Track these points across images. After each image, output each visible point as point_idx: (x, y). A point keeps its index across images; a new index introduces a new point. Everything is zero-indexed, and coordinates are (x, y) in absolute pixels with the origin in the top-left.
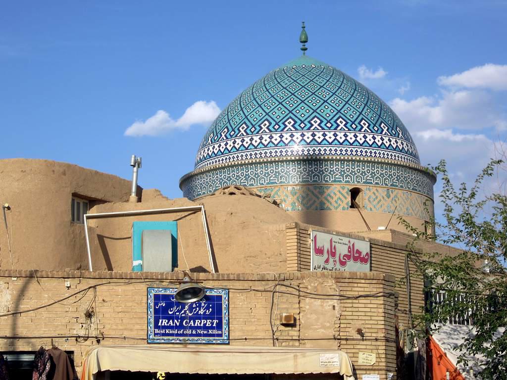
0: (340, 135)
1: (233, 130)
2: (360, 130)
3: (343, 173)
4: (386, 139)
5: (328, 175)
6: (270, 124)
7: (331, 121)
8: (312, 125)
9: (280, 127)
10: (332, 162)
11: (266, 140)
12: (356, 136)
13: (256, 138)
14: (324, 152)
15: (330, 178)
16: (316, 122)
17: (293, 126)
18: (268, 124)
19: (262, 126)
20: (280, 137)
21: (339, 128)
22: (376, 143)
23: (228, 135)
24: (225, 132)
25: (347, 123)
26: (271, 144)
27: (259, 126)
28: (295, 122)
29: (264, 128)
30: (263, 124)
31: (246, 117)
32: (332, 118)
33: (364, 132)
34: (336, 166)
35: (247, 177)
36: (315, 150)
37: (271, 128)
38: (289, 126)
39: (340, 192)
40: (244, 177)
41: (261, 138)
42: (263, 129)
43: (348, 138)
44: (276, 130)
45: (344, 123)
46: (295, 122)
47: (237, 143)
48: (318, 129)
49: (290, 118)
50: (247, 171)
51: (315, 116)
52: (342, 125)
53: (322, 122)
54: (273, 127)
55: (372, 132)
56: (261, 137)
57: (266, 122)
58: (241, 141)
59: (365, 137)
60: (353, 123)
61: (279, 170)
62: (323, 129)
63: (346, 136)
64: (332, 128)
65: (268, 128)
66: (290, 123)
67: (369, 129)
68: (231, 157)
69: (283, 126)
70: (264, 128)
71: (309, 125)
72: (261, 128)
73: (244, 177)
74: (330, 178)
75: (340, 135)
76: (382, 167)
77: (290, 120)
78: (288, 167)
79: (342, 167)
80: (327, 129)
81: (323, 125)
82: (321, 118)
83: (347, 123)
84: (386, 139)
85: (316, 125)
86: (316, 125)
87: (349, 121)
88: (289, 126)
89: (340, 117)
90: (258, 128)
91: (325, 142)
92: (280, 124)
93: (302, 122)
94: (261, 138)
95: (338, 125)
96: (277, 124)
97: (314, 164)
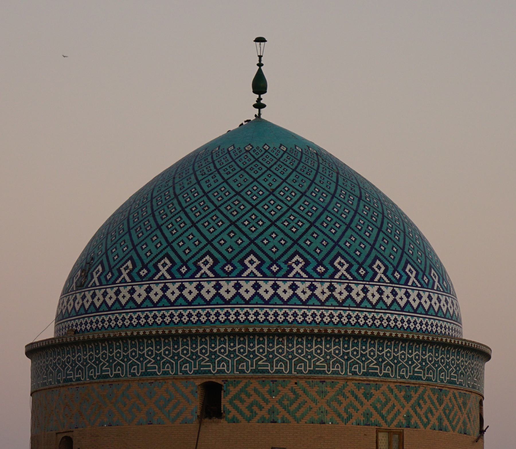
0: (247, 286)
1: (111, 270)
2: (372, 280)
3: (328, 357)
4: (414, 295)
5: (357, 363)
6: (216, 261)
7: (233, 262)
8: (246, 268)
9: (235, 268)
10: (251, 337)
11: (208, 292)
12: (365, 290)
13: (284, 286)
14: (283, 318)
15: (360, 367)
16: (297, 263)
17: (258, 268)
18: (211, 261)
19: (200, 263)
20: (253, 286)
21: (337, 276)
22: (410, 303)
23: (102, 278)
24: (98, 271)
25: (351, 266)
26: (199, 300)
27: (195, 264)
28: (263, 262)
29: (205, 269)
30: (343, 261)
31: (169, 244)
32: (282, 255)
33: (379, 281)
34: (316, 345)
35: (380, 360)
36: (288, 315)
37: (217, 268)
38: (252, 268)
39: (353, 393)
40: (375, 359)
41: (199, 287)
42: (202, 271)
43: (353, 294)
44: (228, 274)
45: (346, 266)
46: (263, 262)
47: (108, 296)
48: (302, 277)
49: (208, 253)
50: (381, 349)
51: (296, 253)
52: (343, 270)
53: (307, 263)
54: (222, 269)
55: (391, 282)
56: (200, 285)
57: (207, 258)
58: (162, 289)
59: (380, 291)
60: (361, 266)
61: (198, 349)
62: (310, 277)
63: (349, 289)
64: (327, 275)
65: (211, 269)
66: (252, 262)
67: (387, 276)
68: (106, 319)
69: (240, 268)
70: (205, 269)
71: (285, 268)
72: (200, 269)
73: (375, 359)
74: (360, 367)
75: (340, 288)
76: (437, 351)
77: (252, 257)
78: (328, 346)
79: (290, 345)
80: (224, 275)
81: (309, 269)
82: (308, 257)
83: (351, 266)
84: (414, 295)
85: (297, 269)
86: (297, 269)
87: (354, 263)
88: (252, 268)
89: (338, 255)
90: (194, 269)
91: (313, 300)
92: (235, 262)
93: (274, 262)
94: (199, 287)
95: (337, 271)
96: (229, 262)
97: (316, 340)
